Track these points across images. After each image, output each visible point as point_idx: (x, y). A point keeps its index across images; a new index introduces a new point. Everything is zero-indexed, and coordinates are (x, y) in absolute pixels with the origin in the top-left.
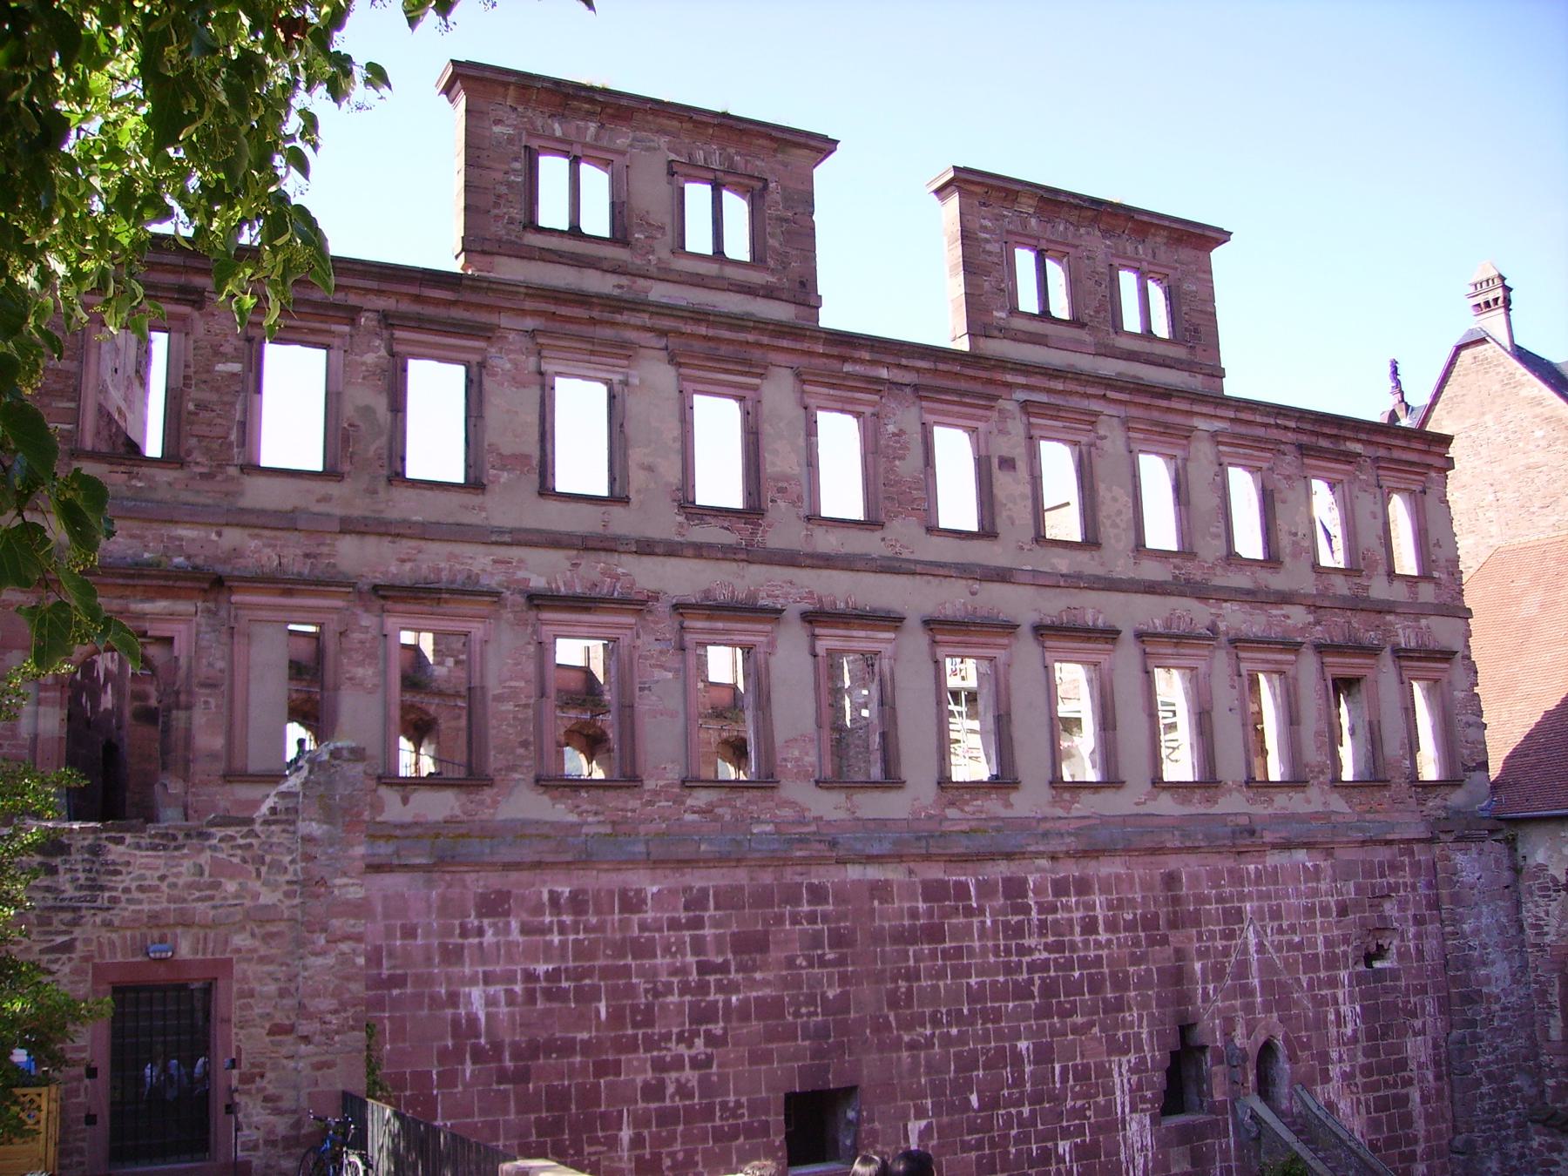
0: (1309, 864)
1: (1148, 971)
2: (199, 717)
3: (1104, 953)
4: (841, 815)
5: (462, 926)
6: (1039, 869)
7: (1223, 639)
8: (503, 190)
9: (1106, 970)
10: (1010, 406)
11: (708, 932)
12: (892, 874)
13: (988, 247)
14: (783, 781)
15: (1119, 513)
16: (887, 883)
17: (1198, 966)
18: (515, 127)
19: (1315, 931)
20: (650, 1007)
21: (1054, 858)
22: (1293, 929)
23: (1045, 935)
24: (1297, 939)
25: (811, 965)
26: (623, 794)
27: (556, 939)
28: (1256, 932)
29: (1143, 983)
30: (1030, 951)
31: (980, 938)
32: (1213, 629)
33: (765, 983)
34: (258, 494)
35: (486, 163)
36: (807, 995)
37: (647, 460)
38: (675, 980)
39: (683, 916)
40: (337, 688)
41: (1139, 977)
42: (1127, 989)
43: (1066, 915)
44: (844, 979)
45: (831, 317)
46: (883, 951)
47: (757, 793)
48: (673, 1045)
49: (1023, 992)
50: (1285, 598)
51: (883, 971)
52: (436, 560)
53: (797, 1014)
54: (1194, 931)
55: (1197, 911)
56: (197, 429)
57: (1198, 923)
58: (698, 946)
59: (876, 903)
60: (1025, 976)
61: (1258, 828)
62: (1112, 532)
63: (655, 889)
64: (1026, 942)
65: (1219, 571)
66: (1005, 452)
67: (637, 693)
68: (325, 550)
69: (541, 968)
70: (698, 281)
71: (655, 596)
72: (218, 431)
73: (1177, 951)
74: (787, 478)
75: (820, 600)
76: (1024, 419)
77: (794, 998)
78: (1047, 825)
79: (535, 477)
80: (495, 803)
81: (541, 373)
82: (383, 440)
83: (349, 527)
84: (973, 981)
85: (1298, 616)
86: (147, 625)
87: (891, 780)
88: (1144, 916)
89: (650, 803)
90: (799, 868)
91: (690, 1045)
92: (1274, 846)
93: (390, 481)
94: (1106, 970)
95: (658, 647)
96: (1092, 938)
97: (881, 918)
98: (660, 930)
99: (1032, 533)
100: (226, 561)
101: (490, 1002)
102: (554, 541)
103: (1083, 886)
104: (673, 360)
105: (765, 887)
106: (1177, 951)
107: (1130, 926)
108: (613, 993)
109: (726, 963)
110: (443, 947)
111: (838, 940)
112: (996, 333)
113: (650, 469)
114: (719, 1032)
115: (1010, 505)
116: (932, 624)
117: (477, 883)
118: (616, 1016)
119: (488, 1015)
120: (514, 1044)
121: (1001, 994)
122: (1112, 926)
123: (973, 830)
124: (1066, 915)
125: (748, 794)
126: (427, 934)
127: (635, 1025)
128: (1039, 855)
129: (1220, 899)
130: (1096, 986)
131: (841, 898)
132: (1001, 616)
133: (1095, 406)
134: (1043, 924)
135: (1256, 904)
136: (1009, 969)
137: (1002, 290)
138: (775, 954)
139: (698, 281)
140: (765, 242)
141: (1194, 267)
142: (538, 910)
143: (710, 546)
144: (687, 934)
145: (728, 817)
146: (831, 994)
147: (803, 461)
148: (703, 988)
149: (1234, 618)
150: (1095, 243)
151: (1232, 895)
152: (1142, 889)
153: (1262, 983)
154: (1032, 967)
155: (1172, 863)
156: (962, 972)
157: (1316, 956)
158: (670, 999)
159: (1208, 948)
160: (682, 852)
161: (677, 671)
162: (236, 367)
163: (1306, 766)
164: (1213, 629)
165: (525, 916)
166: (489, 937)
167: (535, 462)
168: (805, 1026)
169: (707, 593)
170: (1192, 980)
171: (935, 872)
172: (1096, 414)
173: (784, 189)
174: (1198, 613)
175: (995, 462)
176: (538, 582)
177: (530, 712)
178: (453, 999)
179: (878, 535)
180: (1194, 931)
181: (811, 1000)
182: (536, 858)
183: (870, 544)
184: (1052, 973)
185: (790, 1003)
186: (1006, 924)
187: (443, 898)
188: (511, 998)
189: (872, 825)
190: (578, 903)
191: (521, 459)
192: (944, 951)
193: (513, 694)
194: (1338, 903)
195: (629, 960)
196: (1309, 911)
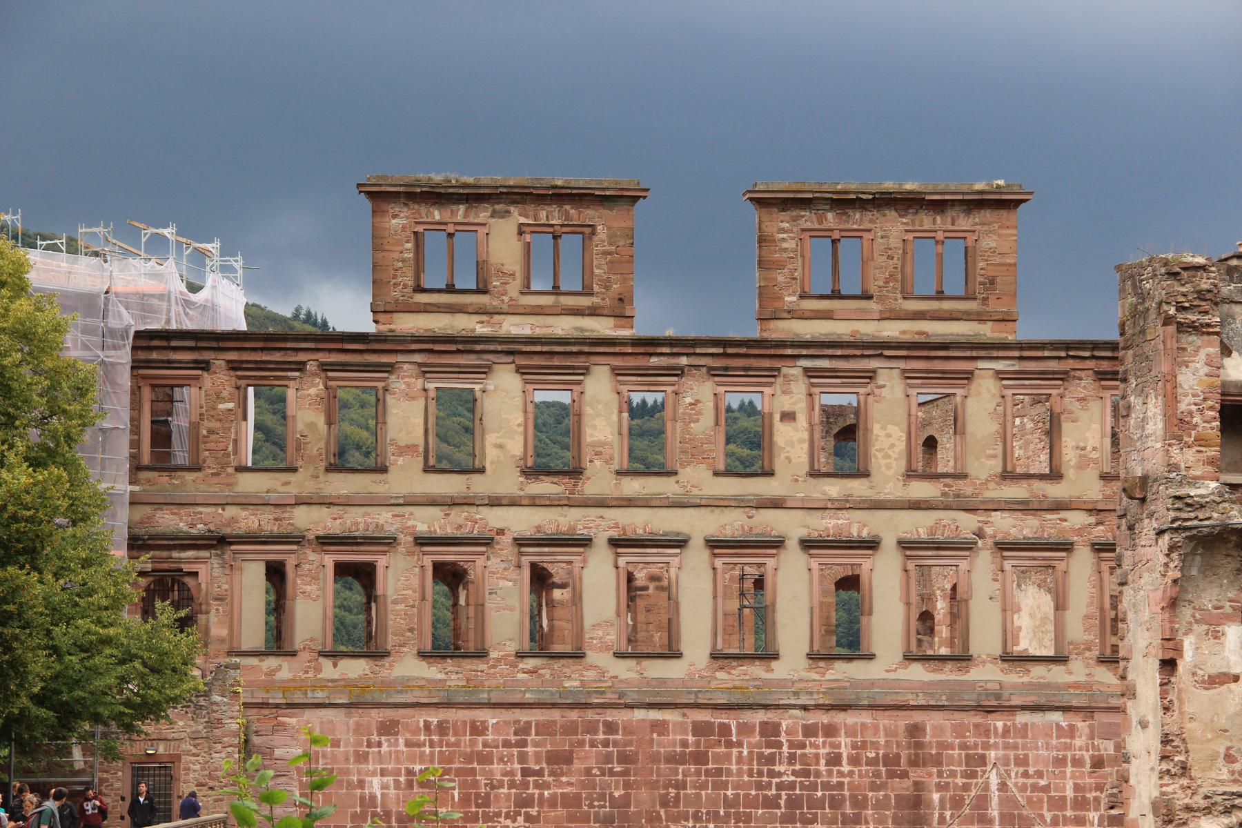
0: (1064, 724)
1: (887, 797)
2: (213, 617)
3: (846, 780)
4: (632, 675)
5: (369, 742)
6: (790, 717)
7: (990, 542)
8: (400, 264)
9: (847, 793)
10: (796, 372)
11: (530, 749)
12: (670, 716)
13: (785, 245)
14: (588, 653)
15: (892, 446)
16: (665, 722)
17: (936, 797)
18: (407, 218)
19: (1064, 778)
20: (488, 795)
21: (805, 708)
22: (1040, 774)
23: (794, 764)
24: (1042, 783)
25: (603, 774)
26: (475, 661)
27: (427, 750)
28: (999, 775)
29: (879, 805)
30: (780, 774)
31: (738, 763)
32: (980, 534)
33: (570, 784)
35: (387, 248)
36: (599, 794)
37: (499, 441)
38: (506, 779)
39: (513, 738)
40: (294, 599)
41: (878, 800)
42: (865, 808)
43: (814, 751)
44: (627, 785)
46: (658, 768)
47: (570, 661)
48: (502, 820)
49: (771, 803)
50: (1059, 506)
51: (657, 781)
52: (355, 521)
53: (591, 806)
54: (935, 770)
55: (939, 755)
56: (212, 446)
57: (940, 764)
58: (523, 758)
59: (655, 735)
60: (774, 792)
61: (1006, 694)
62: (883, 462)
63: (494, 721)
64: (777, 768)
65: (991, 485)
66: (787, 408)
67: (487, 596)
68: (287, 515)
69: (417, 768)
71: (501, 532)
72: (221, 446)
73: (916, 784)
74: (602, 444)
75: (624, 529)
76: (807, 381)
77: (589, 797)
78: (799, 685)
79: (421, 459)
80: (391, 666)
81: (425, 390)
82: (322, 444)
83: (299, 502)
84: (729, 792)
85: (1077, 519)
86: (183, 566)
87: (673, 653)
88: (886, 756)
89: (494, 667)
90: (598, 710)
91: (514, 821)
92: (1024, 708)
93: (327, 470)
94: (847, 793)
95: (503, 565)
96: (835, 769)
97: (659, 745)
98: (497, 747)
99: (806, 468)
100: (228, 525)
101: (384, 787)
102: (433, 502)
103: (830, 731)
104: (517, 371)
105: (572, 722)
106: (916, 784)
107: (870, 762)
108: (463, 785)
109: (542, 770)
110: (356, 752)
111: (624, 758)
112: (785, 315)
113: (500, 446)
114: (535, 813)
115: (788, 448)
116: (714, 545)
117: (376, 715)
118: (465, 800)
119: (382, 795)
120: (399, 813)
121: (752, 803)
122: (854, 761)
123: (735, 688)
124: (814, 751)
125: (563, 661)
126: (346, 745)
127: (477, 806)
128: (794, 707)
129: (963, 746)
130: (836, 803)
131: (628, 730)
132: (774, 533)
133: (873, 364)
134: (792, 759)
135: (1001, 753)
136: (759, 786)
137: (795, 279)
138: (577, 765)
140: (593, 272)
141: (996, 226)
142: (417, 731)
143: (541, 497)
144: (515, 751)
145: (548, 676)
146: (617, 794)
147: (616, 431)
148: (525, 785)
149: (1005, 525)
151: (976, 745)
152: (886, 736)
153: (1002, 816)
154: (780, 787)
155: (917, 717)
156: (724, 786)
157: (1063, 798)
158: (502, 790)
159: (948, 784)
160: (516, 698)
161: (515, 581)
162: (231, 405)
163: (1071, 643)
164: (980, 534)
165: (408, 736)
166: (385, 748)
167: (421, 449)
168: (596, 814)
169: (539, 529)
170: (929, 804)
171: (703, 716)
172: (874, 371)
173: (609, 228)
174: (967, 523)
175: (777, 417)
176: (422, 529)
177: (415, 610)
178: (361, 784)
179: (672, 479)
180: (935, 770)
181: (602, 797)
182: (415, 700)
184: (798, 792)
185: (586, 799)
186: (760, 756)
187: (357, 724)
188: (397, 785)
189: (654, 683)
190: (442, 728)
191: (411, 448)
192: (706, 770)
193: (405, 598)
194: (1092, 757)
195: (475, 765)
196: (1060, 762)
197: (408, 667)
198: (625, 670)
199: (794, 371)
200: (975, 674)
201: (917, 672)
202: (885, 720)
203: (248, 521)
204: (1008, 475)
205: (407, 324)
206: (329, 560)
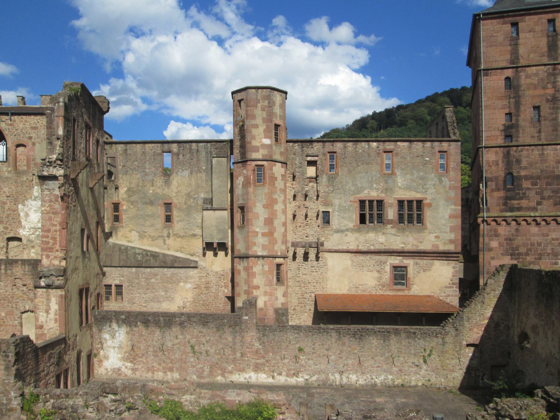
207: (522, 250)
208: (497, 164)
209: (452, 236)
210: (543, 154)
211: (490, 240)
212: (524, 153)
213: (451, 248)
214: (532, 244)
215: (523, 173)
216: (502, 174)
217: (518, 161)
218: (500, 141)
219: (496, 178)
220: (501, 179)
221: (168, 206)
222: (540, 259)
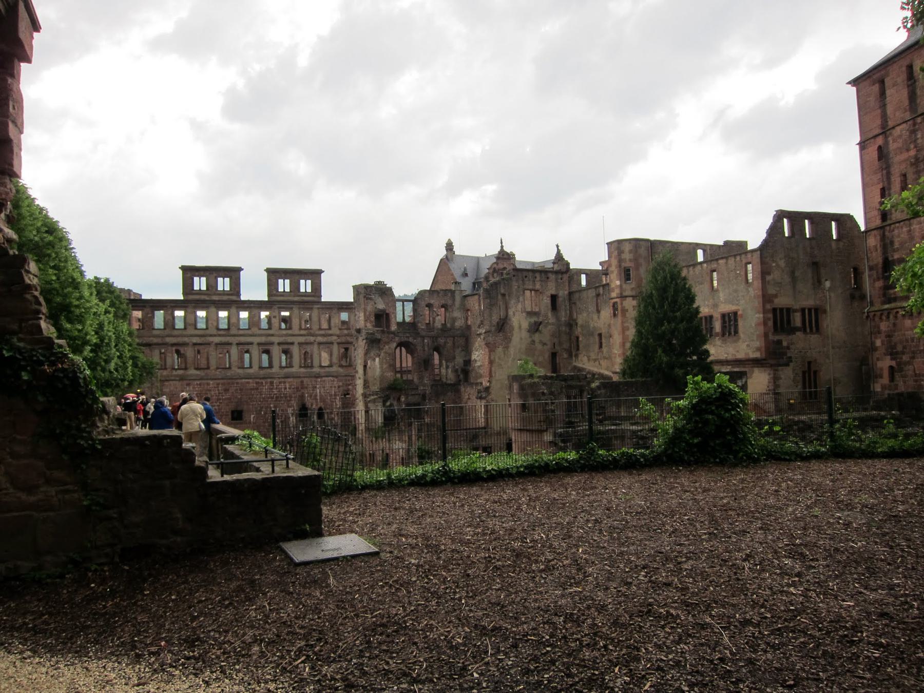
12: (250, 381)
34: (155, 332)
45: (243, 298)
50: (331, 335)
52: (180, 340)
70: (220, 294)
83: (168, 336)
85: (335, 338)
103: (285, 382)
111: (241, 390)
116: (259, 344)
117: (185, 382)
139: (220, 294)
149: (320, 339)
150: (297, 277)
174: (312, 339)
183: (249, 332)
197: (192, 372)
198: (240, 371)
199: (276, 307)
200: (314, 370)
201: (303, 370)
202: (295, 380)
203: (155, 340)
204: (320, 329)
205: (191, 297)
206: (174, 349)
207: (899, 348)
208: (877, 250)
209: (757, 344)
210: (910, 231)
211: (876, 338)
212: (896, 232)
213: (757, 355)
214: (907, 341)
215: (896, 256)
216: (880, 260)
217: (892, 243)
218: (878, 222)
219: (877, 265)
220: (880, 266)
221: (600, 335)
222: (913, 358)
